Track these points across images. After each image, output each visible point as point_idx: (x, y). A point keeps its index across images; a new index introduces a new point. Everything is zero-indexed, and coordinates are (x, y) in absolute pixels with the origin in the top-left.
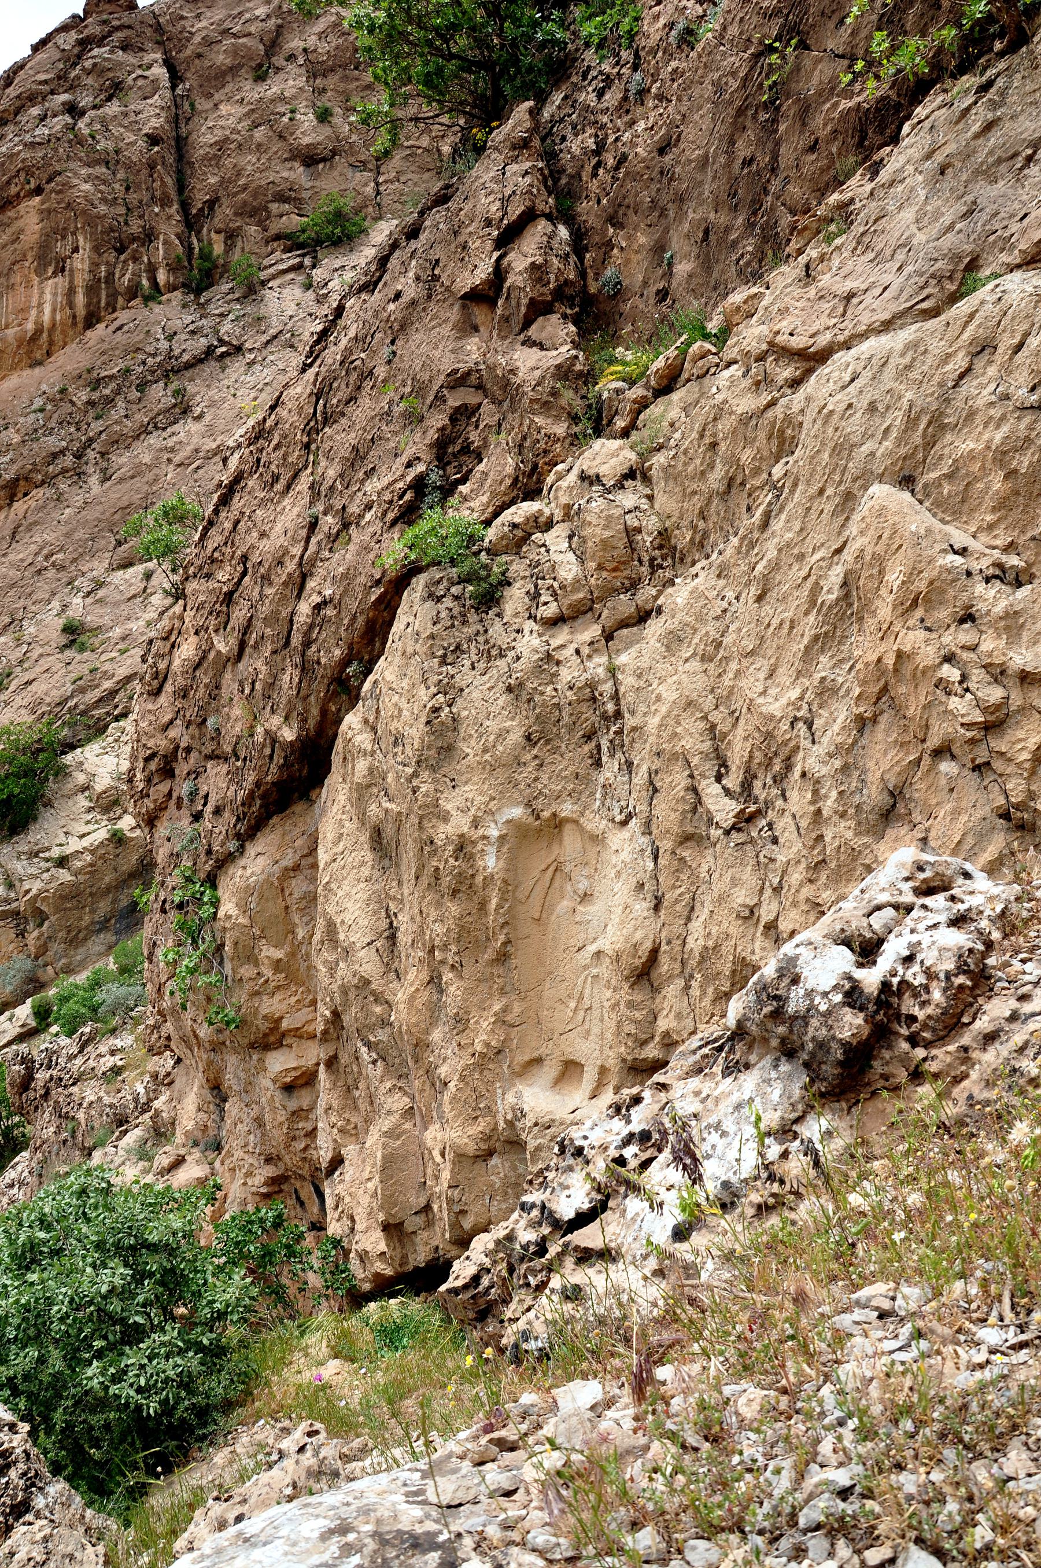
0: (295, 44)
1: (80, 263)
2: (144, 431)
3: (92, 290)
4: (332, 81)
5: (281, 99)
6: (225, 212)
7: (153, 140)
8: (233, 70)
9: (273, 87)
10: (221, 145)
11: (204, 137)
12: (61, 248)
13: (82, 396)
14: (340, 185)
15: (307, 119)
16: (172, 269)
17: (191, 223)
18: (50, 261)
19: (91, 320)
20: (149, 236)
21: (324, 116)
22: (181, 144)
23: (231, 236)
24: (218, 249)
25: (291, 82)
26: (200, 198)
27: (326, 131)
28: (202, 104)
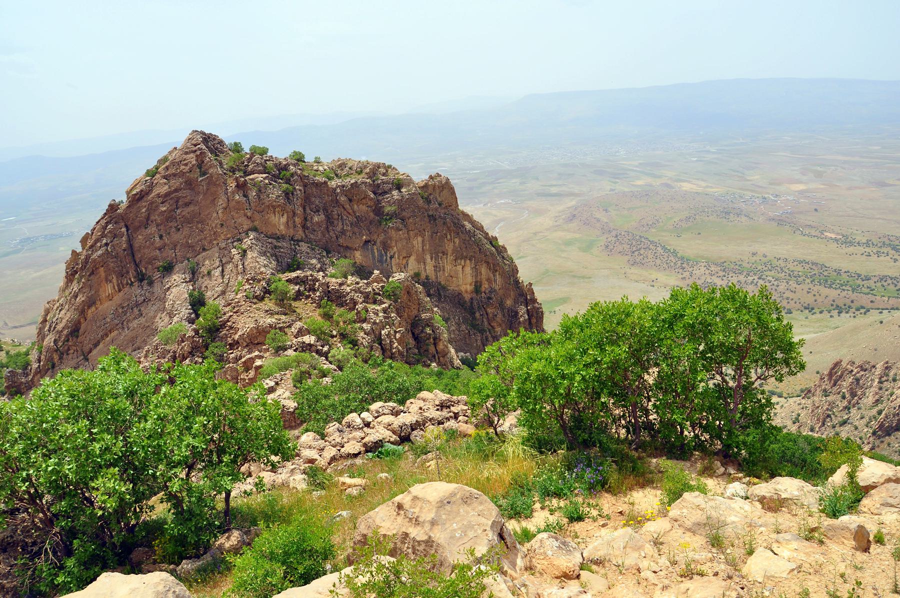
0: (152, 218)
1: (115, 281)
2: (135, 318)
3: (118, 285)
4: (162, 227)
5: (151, 234)
6: (143, 263)
7: (124, 250)
8: (140, 227)
9: (149, 231)
10: (140, 247)
11: (136, 245)
12: (110, 278)
13: (120, 310)
14: (170, 254)
15: (157, 239)
16: (135, 277)
17: (137, 265)
18: (107, 280)
19: (120, 291)
20: (128, 272)
21: (161, 237)
22: (131, 246)
23: (146, 268)
24: (144, 271)
25: (152, 229)
26: (138, 261)
27: (162, 242)
28: (135, 236)
